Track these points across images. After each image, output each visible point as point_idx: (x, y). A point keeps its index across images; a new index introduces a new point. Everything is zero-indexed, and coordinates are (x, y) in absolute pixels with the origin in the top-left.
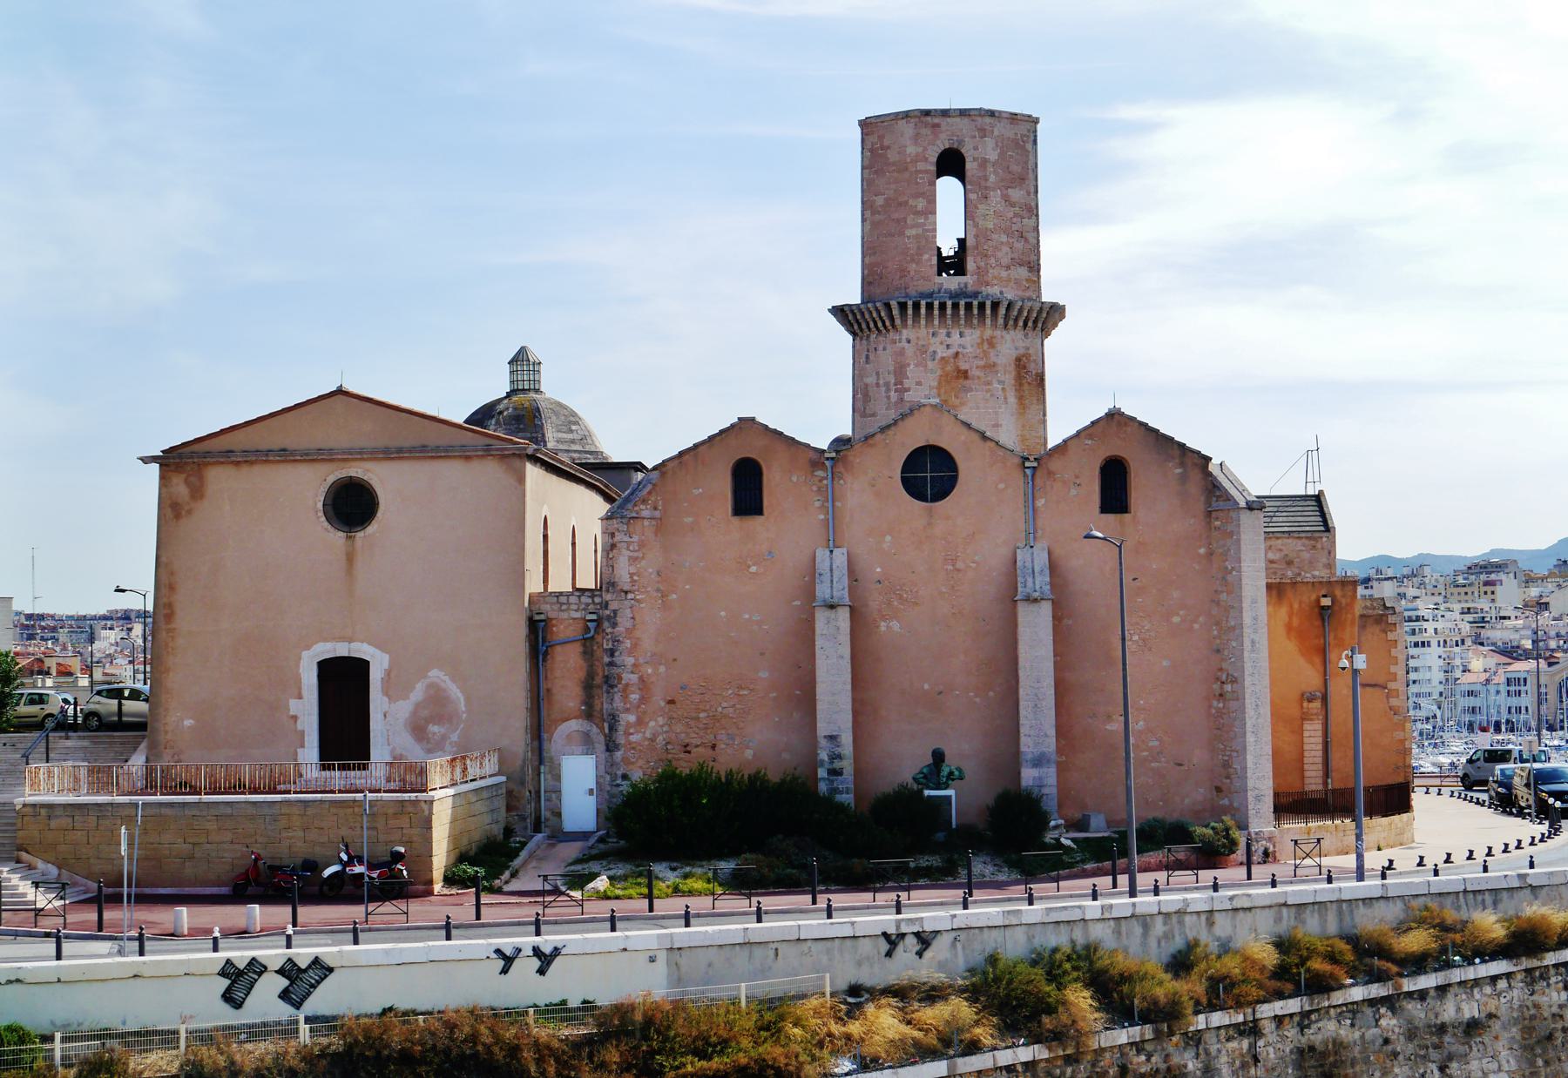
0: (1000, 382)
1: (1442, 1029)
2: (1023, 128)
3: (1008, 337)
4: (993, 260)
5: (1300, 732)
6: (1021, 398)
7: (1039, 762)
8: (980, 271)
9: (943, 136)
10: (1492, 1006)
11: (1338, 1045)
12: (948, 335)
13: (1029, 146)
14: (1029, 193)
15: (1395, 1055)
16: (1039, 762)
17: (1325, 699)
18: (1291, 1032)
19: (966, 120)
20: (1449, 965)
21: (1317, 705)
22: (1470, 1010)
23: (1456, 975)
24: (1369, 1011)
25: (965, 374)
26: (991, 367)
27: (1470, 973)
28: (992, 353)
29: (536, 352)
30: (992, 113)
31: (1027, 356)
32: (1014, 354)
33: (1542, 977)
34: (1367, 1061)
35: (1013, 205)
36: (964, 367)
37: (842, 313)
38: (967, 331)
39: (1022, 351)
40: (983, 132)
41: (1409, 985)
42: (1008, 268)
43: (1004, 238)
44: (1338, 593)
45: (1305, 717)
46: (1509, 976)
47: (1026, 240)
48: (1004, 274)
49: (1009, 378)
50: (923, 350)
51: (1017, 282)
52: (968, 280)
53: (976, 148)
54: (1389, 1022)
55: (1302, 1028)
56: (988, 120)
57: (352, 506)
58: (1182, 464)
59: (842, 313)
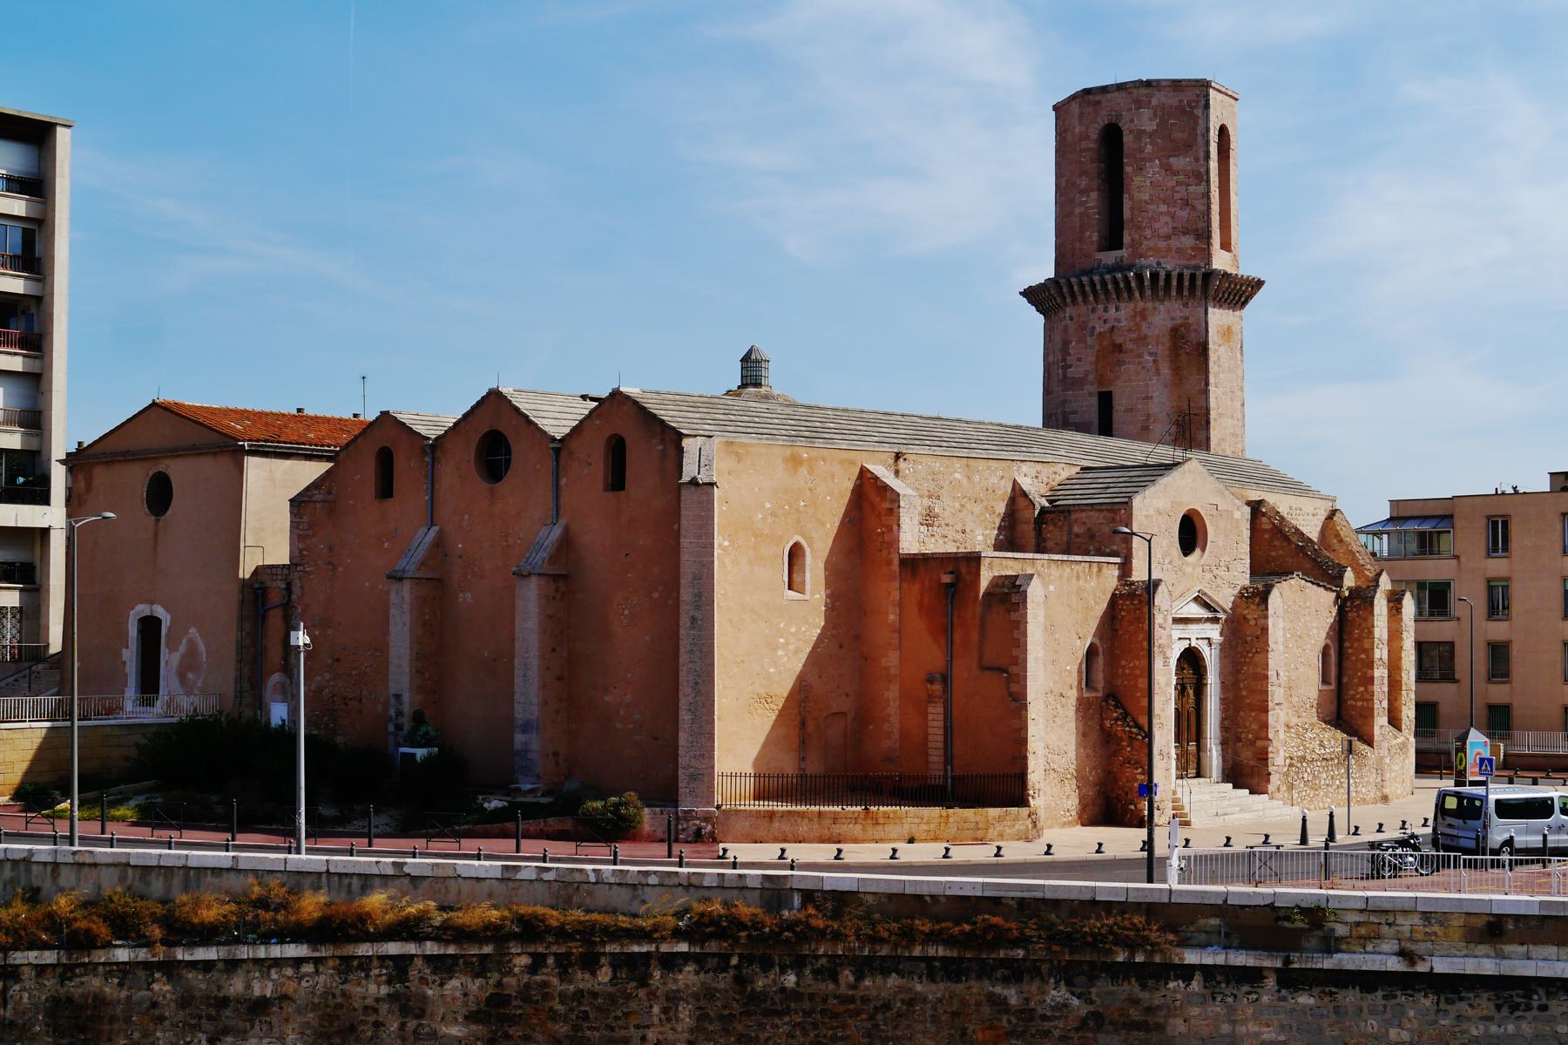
0: (1150, 354)
1: (224, 1002)
2: (1187, 96)
3: (1162, 308)
4: (1148, 232)
5: (924, 714)
6: (1176, 369)
7: (526, 727)
8: (1135, 244)
9: (1103, 113)
10: (290, 987)
11: (99, 1000)
12: (1106, 310)
13: (1199, 112)
14: (1197, 160)
15: (162, 1019)
16: (526, 727)
17: (945, 680)
18: (50, 982)
19: (1123, 94)
20: (238, 941)
21: (937, 687)
22: (262, 988)
23: (244, 952)
24: (142, 974)
25: (1119, 348)
26: (1142, 340)
27: (261, 952)
28: (1144, 325)
29: (765, 351)
30: (1149, 83)
31: (1186, 326)
32: (1169, 324)
33: (360, 967)
34: (128, 1020)
35: (1177, 173)
36: (1119, 340)
37: (1031, 294)
38: (1122, 305)
39: (1179, 322)
40: (1139, 104)
41: (244, 952)
42: (1168, 237)
43: (1163, 208)
44: (964, 570)
45: (930, 699)
46: (317, 961)
47: (1194, 208)
48: (1162, 244)
49: (1163, 350)
50: (1083, 326)
51: (1179, 251)
52: (1124, 253)
53: (1132, 121)
54: (161, 987)
55: (63, 979)
56: (1144, 91)
57: (160, 495)
58: (663, 441)
59: (1031, 294)
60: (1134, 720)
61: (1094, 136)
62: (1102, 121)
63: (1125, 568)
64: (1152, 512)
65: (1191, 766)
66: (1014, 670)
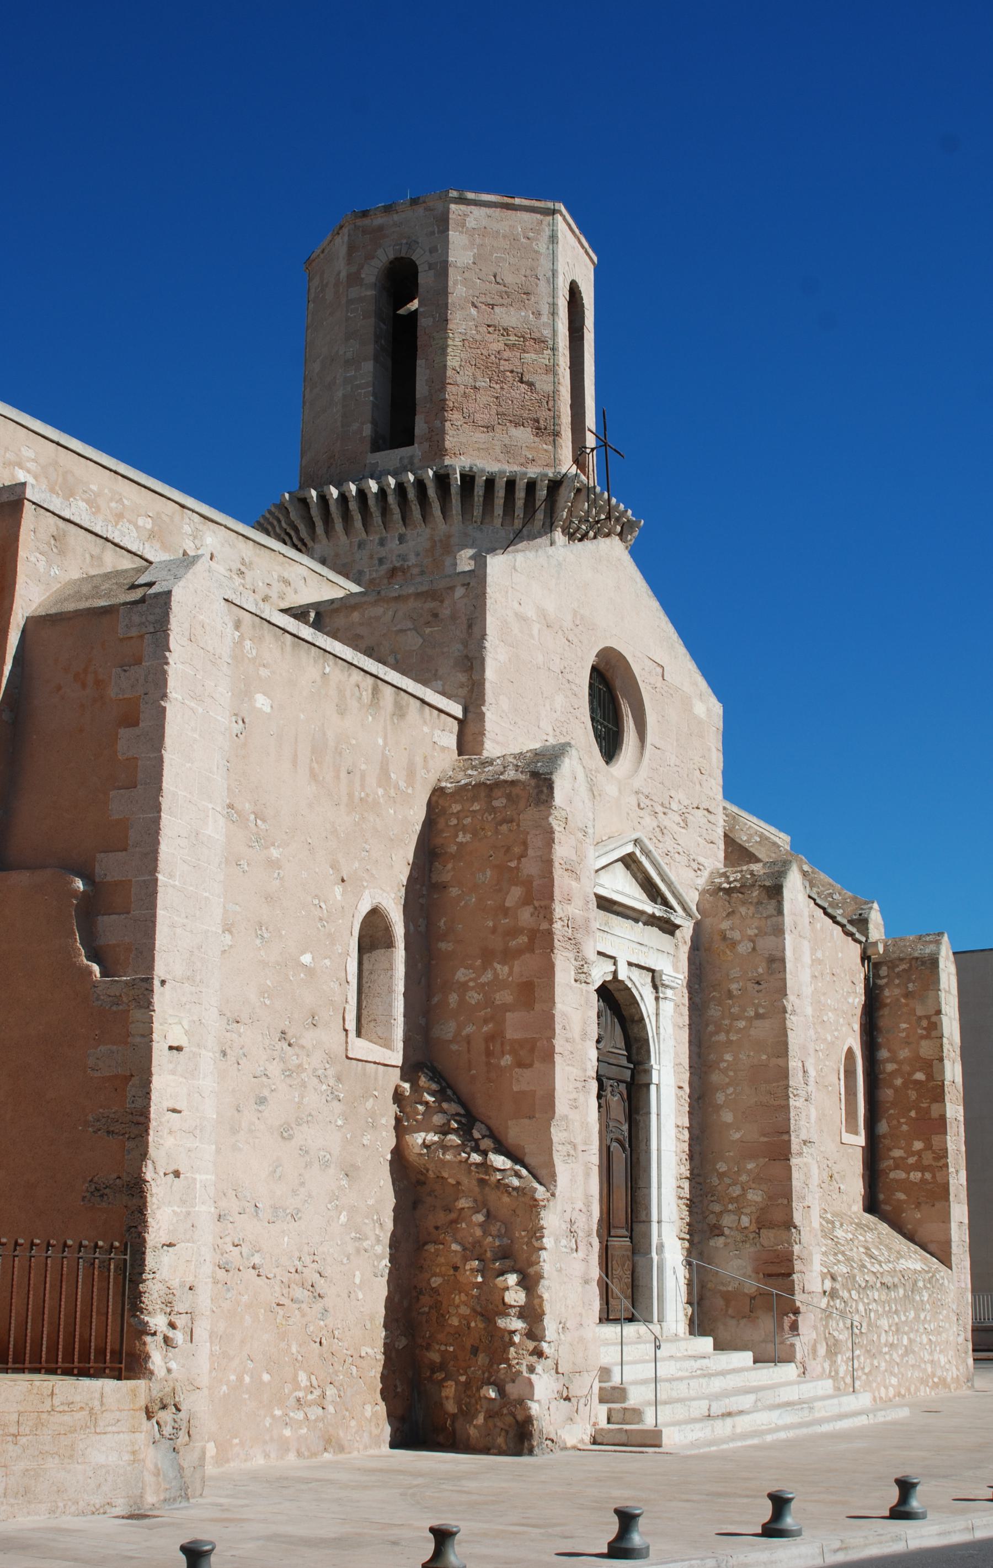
12: (382, 542)
60: (492, 1135)
61: (372, 279)
62: (384, 256)
63: (469, 734)
64: (531, 613)
65: (625, 1295)
66: (110, 867)
